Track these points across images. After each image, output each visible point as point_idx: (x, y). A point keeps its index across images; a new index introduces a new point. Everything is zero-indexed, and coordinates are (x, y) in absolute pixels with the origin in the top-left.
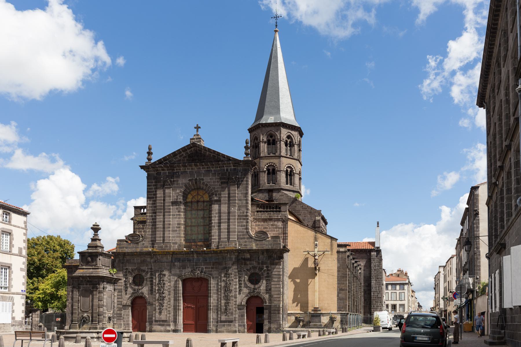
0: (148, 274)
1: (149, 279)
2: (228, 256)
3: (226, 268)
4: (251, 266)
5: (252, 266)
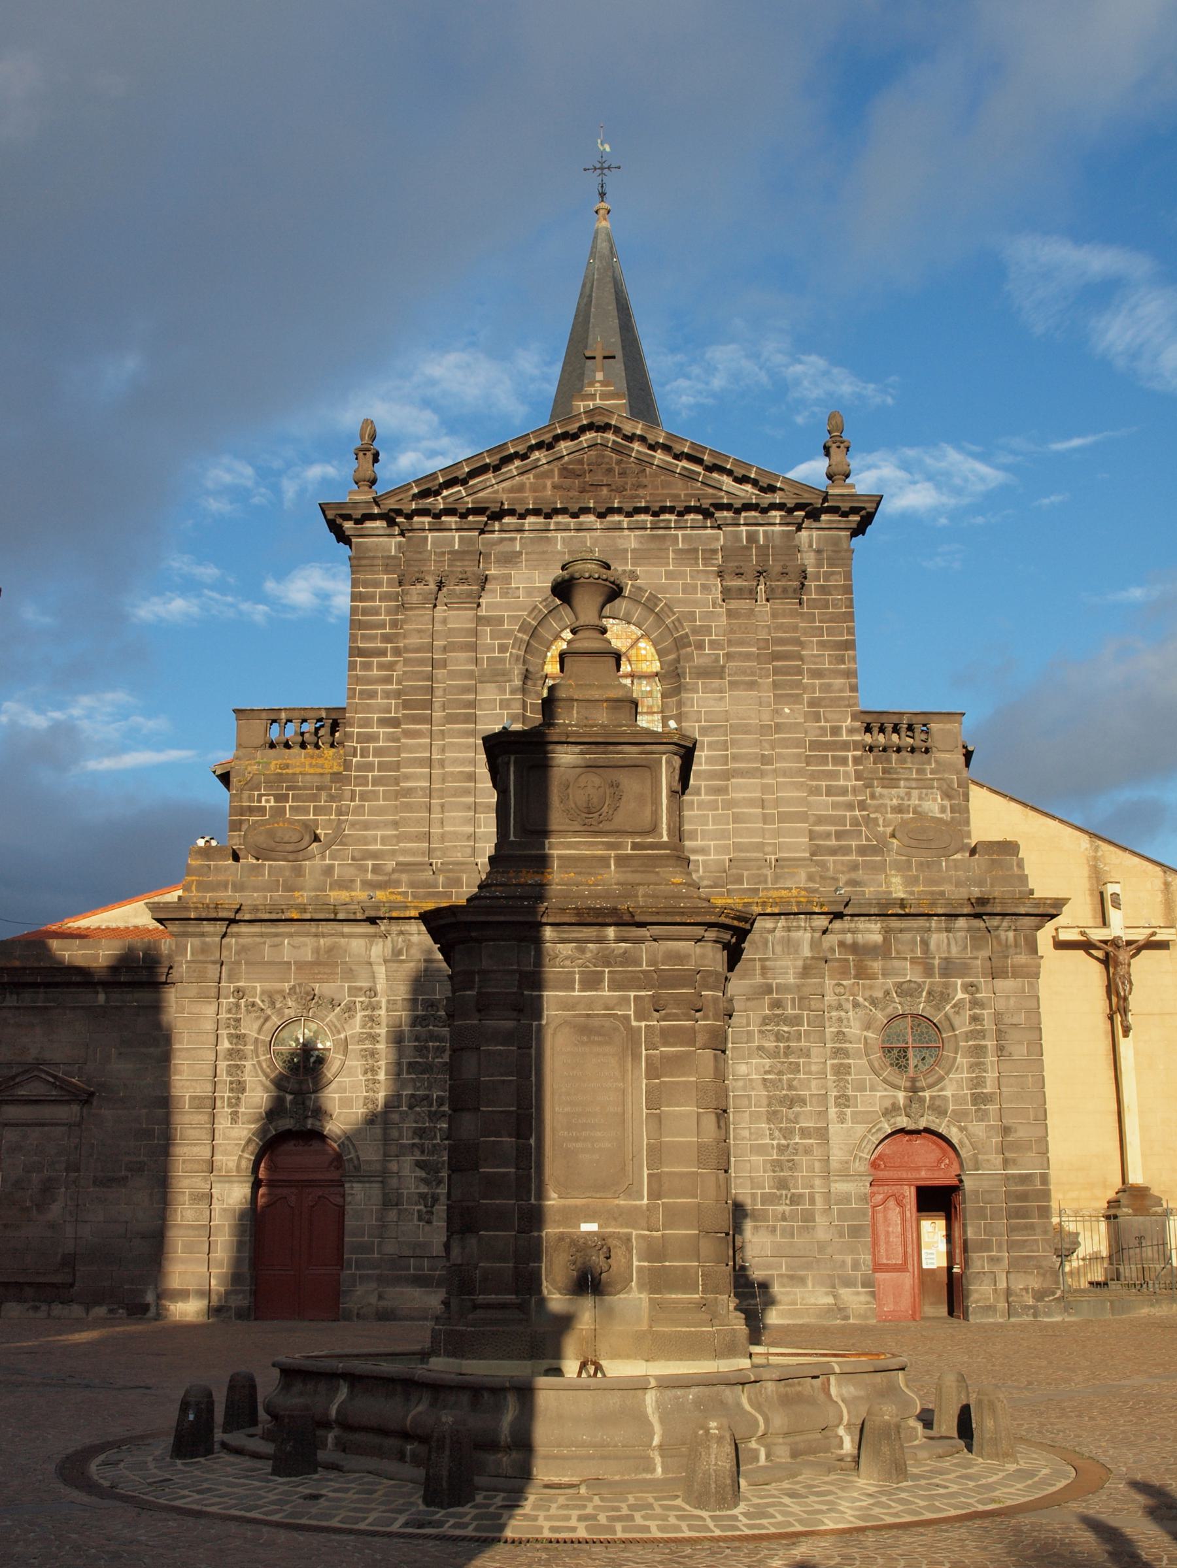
0: (352, 1017)
1: (361, 1041)
2: (779, 934)
3: (769, 990)
4: (890, 982)
5: (899, 985)
